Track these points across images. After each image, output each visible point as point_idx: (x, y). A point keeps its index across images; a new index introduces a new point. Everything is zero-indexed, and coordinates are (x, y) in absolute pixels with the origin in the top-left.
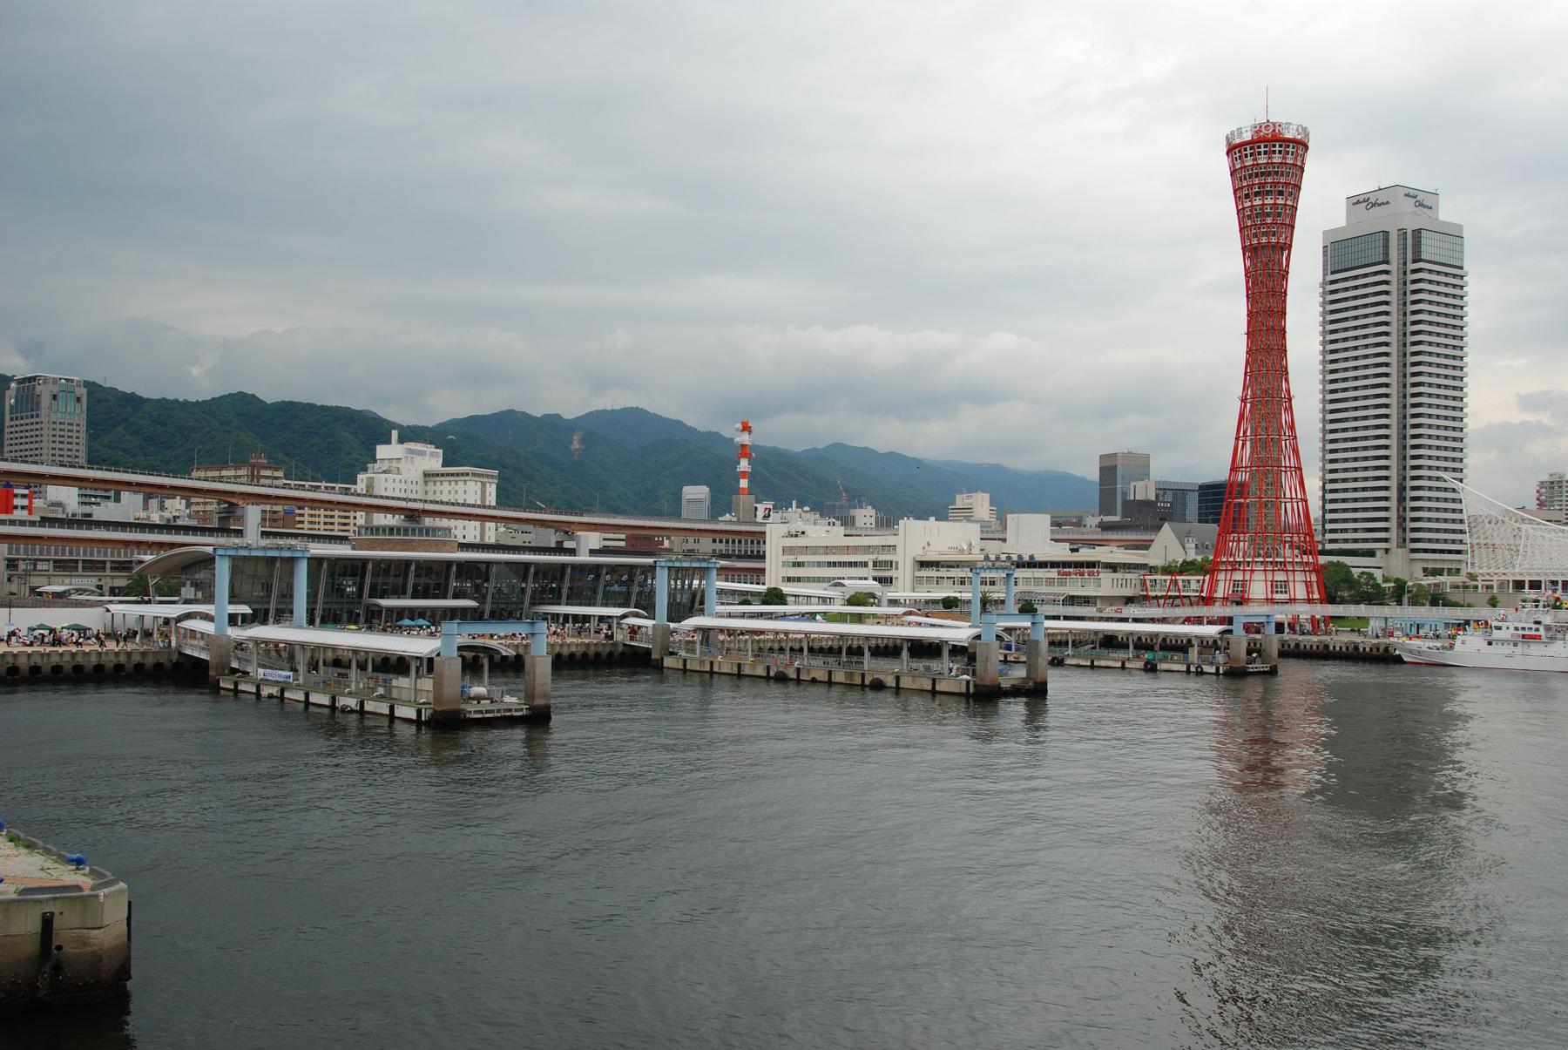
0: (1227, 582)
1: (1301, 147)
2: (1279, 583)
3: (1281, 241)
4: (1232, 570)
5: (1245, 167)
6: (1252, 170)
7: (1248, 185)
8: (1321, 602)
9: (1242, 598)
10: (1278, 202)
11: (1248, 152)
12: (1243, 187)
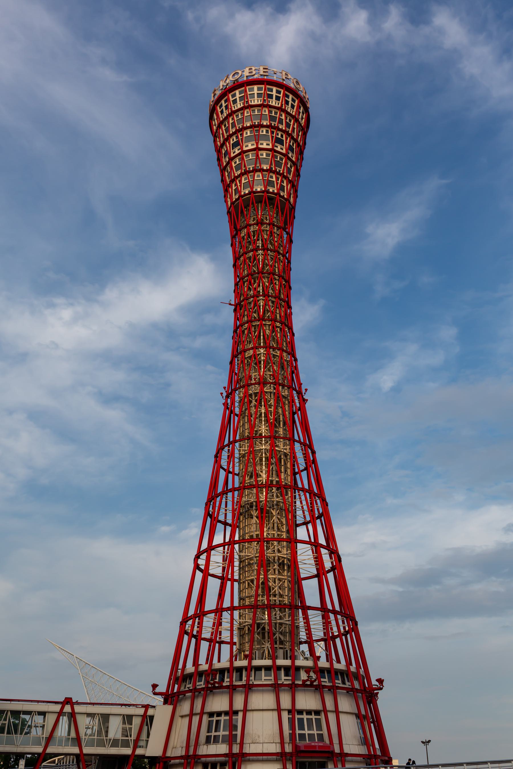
0: (196, 720)
2: (305, 717)
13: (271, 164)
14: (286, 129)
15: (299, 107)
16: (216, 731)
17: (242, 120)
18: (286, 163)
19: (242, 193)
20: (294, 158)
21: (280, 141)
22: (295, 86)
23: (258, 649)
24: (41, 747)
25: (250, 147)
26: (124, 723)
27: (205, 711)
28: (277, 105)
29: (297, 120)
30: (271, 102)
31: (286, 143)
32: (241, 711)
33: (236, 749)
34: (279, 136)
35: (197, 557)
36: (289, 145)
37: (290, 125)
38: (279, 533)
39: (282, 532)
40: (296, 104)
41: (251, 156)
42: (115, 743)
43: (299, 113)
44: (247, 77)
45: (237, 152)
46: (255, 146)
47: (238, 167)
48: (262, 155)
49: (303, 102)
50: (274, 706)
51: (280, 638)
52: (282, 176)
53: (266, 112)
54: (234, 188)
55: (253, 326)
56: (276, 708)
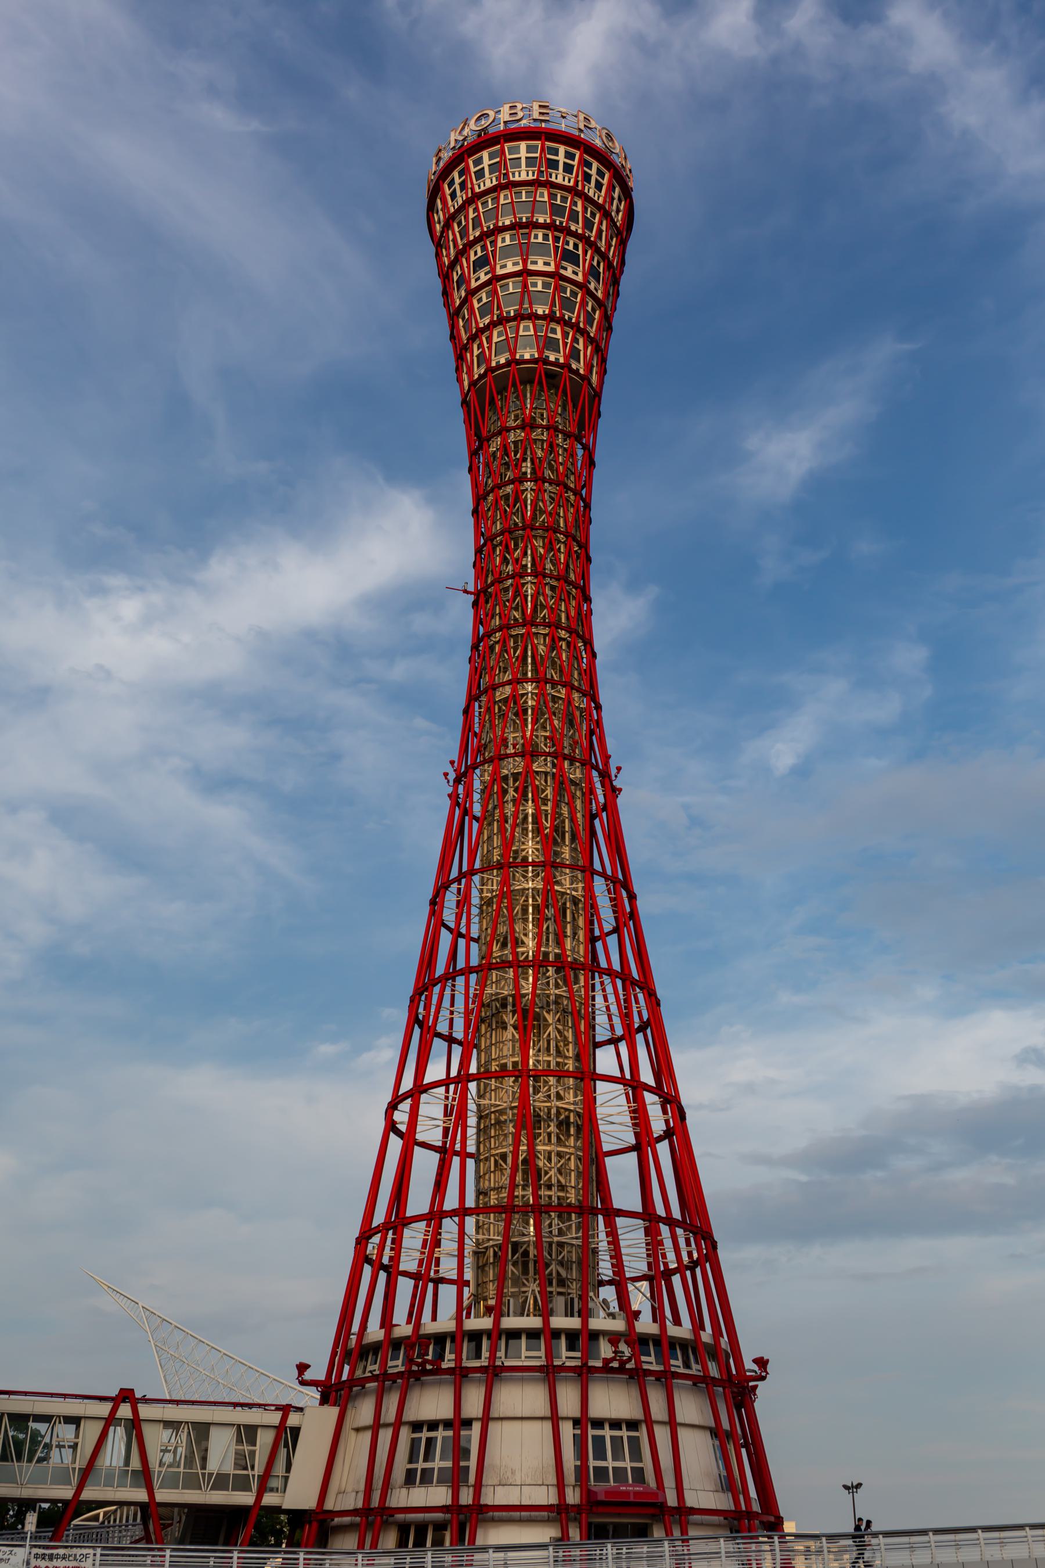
0: (385, 1436)
2: (607, 1433)
13: (553, 304)
14: (584, 232)
15: (611, 188)
16: (425, 1460)
17: (495, 212)
18: (584, 303)
19: (494, 364)
20: (599, 292)
21: (572, 258)
22: (604, 144)
23: (513, 1295)
24: (69, 1487)
25: (510, 268)
26: (239, 1441)
27: (405, 1418)
28: (566, 183)
29: (606, 215)
30: (554, 176)
31: (585, 260)
32: (477, 1419)
33: (466, 1497)
34: (571, 247)
35: (392, 1107)
36: (591, 265)
37: (594, 223)
38: (559, 1060)
39: (566, 1057)
40: (605, 181)
41: (512, 287)
42: (221, 1482)
43: (613, 199)
44: (505, 122)
45: (484, 278)
46: (520, 267)
47: (485, 310)
48: (535, 285)
49: (620, 178)
50: (544, 1410)
51: (558, 1274)
52: (575, 328)
53: (543, 194)
54: (476, 352)
55: (512, 636)
56: (548, 1414)
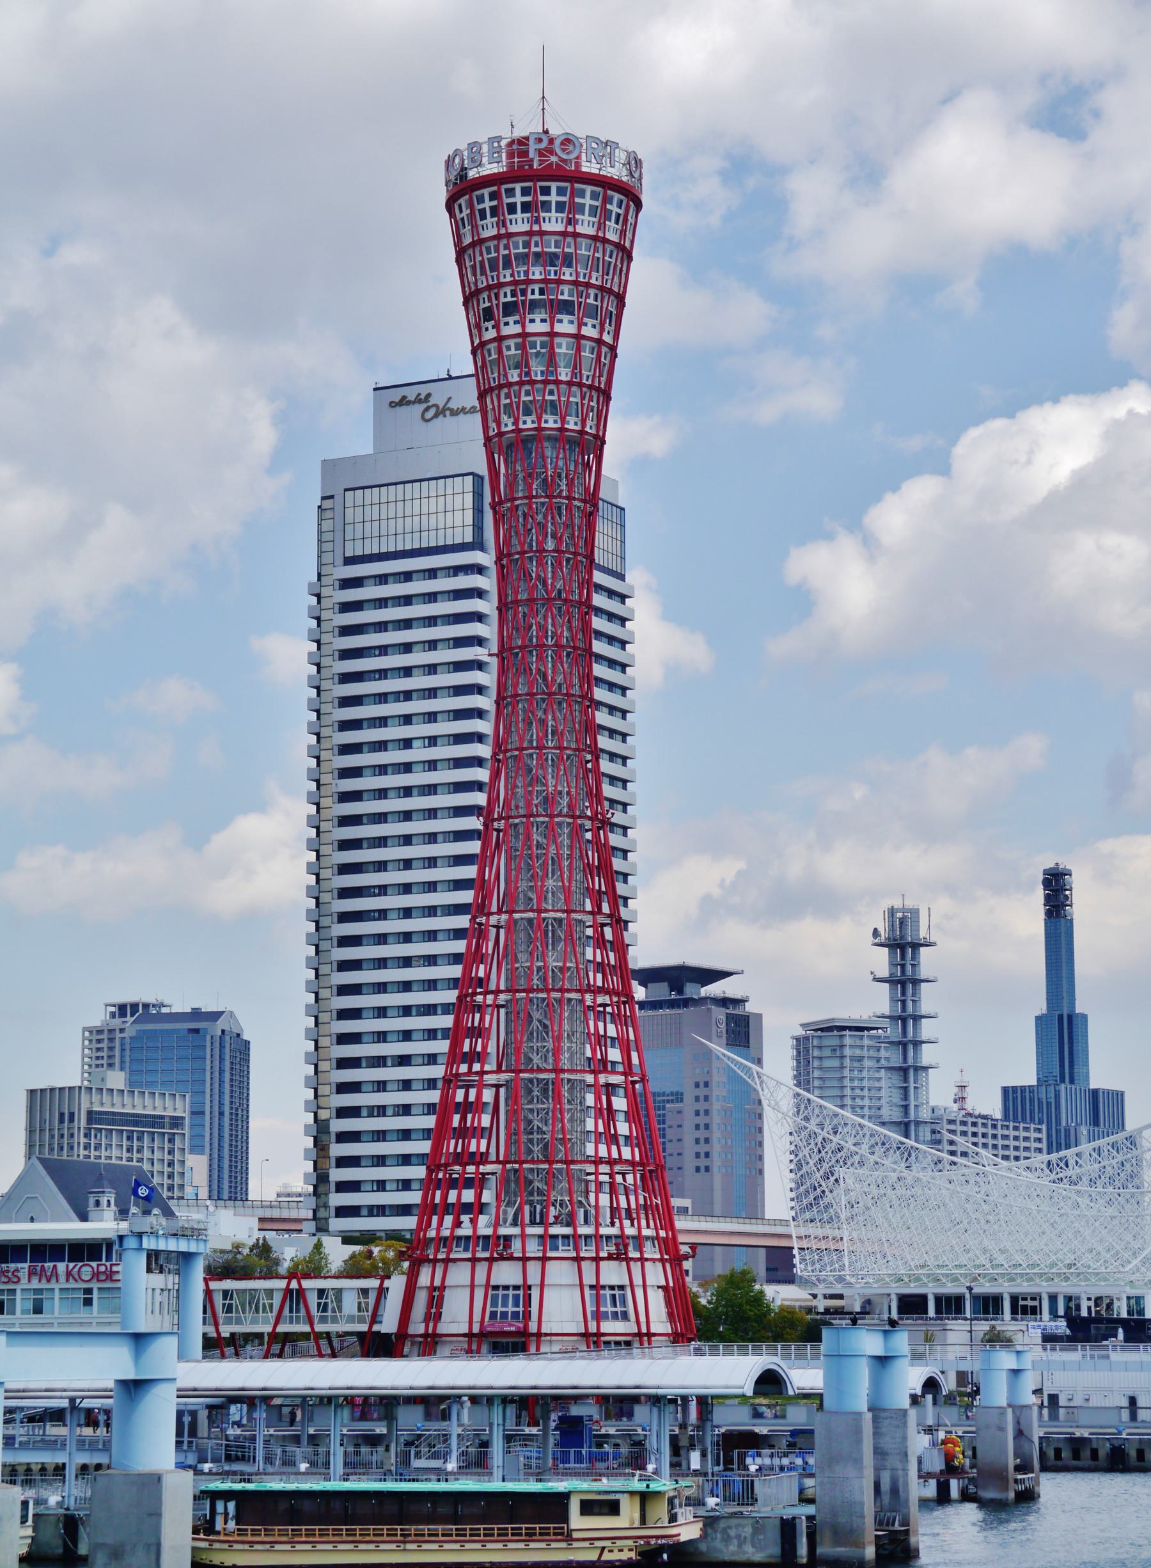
1: (617, 197)
2: (608, 1292)
3: (588, 429)
4: (491, 1260)
5: (509, 235)
6: (527, 245)
7: (515, 283)
8: (678, 1338)
9: (524, 1333)
10: (558, 328)
11: (519, 199)
12: (500, 285)
42: (351, 1319)
